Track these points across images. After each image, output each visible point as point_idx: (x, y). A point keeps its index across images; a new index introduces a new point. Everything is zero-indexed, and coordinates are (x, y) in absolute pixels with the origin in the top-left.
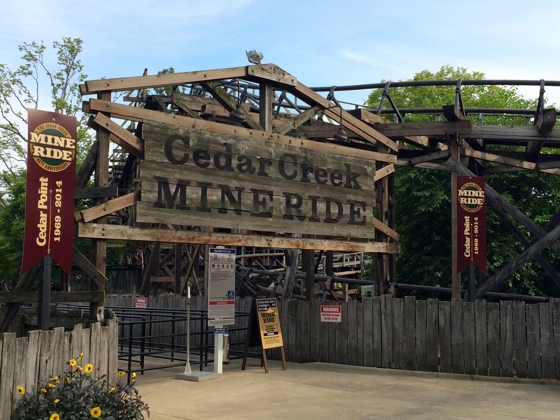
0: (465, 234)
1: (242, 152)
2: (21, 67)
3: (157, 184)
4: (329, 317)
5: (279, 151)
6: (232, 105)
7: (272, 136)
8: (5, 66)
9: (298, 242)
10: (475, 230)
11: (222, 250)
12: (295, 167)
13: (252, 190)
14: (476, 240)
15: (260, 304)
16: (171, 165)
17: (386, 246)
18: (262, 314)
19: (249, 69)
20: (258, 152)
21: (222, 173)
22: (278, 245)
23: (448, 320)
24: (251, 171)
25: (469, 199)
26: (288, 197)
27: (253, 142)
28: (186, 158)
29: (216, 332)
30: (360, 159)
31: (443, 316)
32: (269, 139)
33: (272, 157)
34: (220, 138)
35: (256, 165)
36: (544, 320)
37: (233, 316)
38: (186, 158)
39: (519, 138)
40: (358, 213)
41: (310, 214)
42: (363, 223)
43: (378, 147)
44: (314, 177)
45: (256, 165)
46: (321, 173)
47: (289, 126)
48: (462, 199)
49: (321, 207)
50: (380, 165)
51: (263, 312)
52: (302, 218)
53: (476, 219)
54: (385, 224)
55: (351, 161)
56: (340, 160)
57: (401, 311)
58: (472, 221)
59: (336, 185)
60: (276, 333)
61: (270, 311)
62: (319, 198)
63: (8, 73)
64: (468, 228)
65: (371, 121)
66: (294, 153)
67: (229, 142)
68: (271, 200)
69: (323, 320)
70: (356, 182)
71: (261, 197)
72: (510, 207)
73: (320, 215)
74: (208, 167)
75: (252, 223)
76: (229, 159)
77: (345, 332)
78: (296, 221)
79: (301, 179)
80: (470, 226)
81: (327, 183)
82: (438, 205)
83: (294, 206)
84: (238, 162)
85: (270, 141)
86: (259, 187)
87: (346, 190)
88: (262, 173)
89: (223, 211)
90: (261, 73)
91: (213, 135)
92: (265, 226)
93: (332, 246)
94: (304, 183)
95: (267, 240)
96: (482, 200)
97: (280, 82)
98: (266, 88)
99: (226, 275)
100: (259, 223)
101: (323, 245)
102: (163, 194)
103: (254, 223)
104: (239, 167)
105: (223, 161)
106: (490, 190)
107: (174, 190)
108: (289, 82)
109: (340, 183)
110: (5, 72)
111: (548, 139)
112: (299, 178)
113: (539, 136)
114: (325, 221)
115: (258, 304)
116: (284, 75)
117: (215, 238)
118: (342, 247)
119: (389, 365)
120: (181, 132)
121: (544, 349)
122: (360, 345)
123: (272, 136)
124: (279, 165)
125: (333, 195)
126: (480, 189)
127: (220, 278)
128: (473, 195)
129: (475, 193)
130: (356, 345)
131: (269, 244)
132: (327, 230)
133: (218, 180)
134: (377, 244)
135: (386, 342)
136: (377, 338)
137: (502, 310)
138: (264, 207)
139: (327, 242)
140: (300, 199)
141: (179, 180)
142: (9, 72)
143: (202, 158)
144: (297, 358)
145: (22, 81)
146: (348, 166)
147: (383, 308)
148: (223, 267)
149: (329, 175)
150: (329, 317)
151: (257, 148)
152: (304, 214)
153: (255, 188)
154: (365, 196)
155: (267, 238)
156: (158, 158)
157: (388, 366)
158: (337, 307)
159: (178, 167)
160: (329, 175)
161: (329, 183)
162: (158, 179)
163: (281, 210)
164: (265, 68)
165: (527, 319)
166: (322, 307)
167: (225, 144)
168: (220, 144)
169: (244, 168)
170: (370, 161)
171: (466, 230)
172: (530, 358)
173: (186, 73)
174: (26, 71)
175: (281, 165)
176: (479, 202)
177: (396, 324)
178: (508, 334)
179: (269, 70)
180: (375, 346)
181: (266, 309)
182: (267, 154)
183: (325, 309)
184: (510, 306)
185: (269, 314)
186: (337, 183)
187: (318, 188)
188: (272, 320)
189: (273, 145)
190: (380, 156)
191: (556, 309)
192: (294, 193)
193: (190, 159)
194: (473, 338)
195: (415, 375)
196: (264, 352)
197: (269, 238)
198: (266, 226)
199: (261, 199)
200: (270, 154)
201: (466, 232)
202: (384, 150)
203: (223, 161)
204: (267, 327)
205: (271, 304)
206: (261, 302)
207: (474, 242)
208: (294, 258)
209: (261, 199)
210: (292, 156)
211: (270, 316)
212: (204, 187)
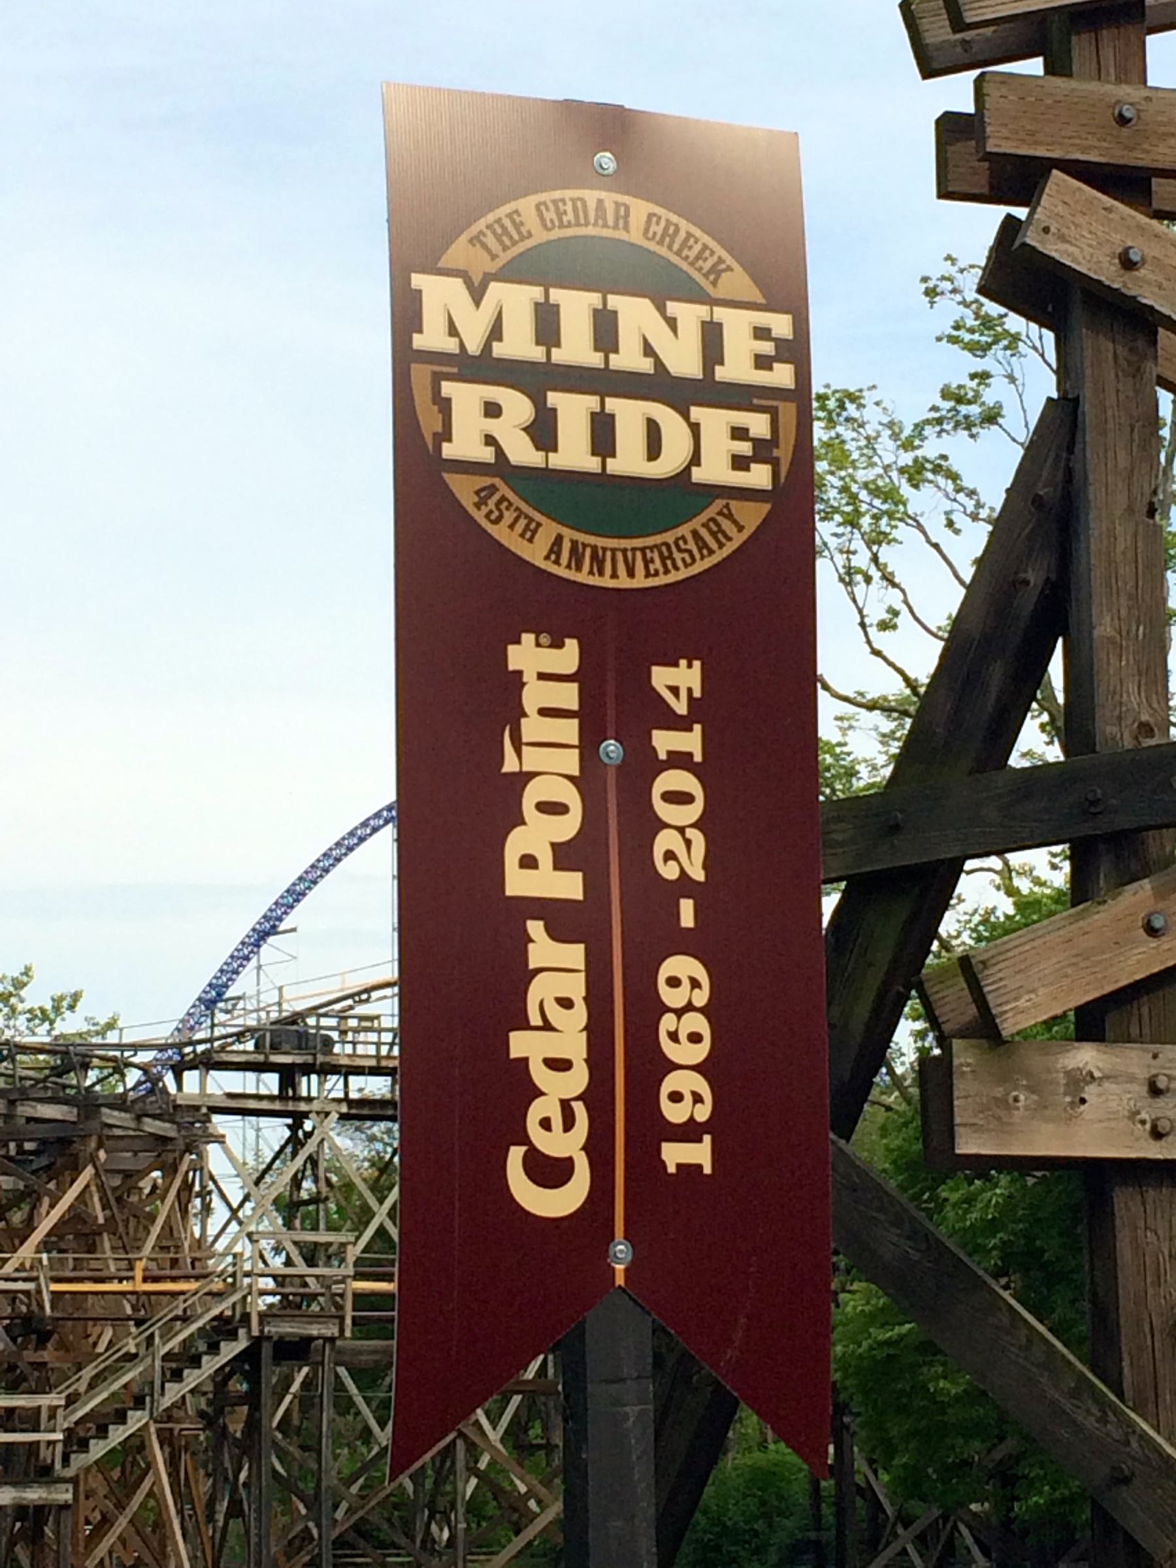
0: (518, 883)
10: (665, 841)
96: (759, 424)
128: (630, 358)
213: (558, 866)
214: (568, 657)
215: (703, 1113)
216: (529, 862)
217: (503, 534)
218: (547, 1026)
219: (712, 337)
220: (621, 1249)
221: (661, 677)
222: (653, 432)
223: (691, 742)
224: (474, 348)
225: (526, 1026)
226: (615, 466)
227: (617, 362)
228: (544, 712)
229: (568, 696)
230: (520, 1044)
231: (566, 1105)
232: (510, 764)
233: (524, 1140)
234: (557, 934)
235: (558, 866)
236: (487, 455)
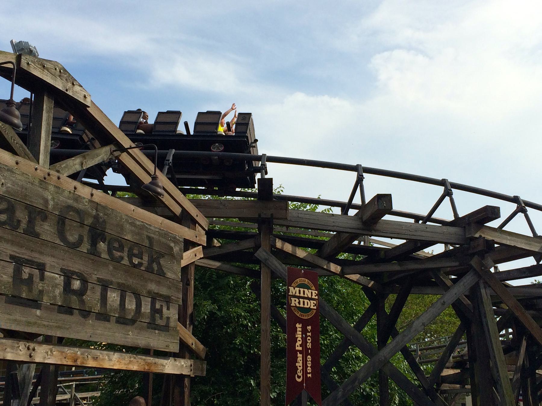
0: (297, 348)
5: (59, 200)
9: (76, 353)
10: (308, 344)
13: (12, 257)
17: (190, 365)
19: (22, 60)
22: (45, 358)
26: (68, 276)
32: (45, 178)
35: (22, 215)
40: (160, 311)
41: (97, 308)
42: (166, 328)
44: (106, 249)
45: (22, 215)
46: (116, 245)
47: (74, 165)
48: (293, 299)
49: (113, 297)
53: (309, 328)
54: (189, 331)
56: (141, 229)
58: (304, 331)
59: (135, 266)
62: (111, 283)
64: (299, 341)
66: (80, 206)
68: (42, 278)
70: (159, 264)
71: (26, 271)
75: (8, 316)
78: (76, 317)
79: (88, 250)
80: (302, 338)
81: (122, 262)
82: (206, 317)
83: (74, 292)
86: (24, 254)
87: (147, 275)
88: (30, 232)
92: (29, 324)
93: (123, 362)
94: (92, 257)
95: (28, 349)
96: (315, 302)
97: (68, 93)
98: (45, 98)
100: (18, 316)
103: (11, 317)
108: (80, 98)
109: (140, 264)
112: (85, 248)
113: (363, 229)
116: (73, 84)
118: (137, 364)
123: (49, 175)
124: (58, 223)
125: (131, 281)
126: (313, 288)
128: (306, 296)
129: (308, 293)
131: (31, 356)
134: (180, 362)
138: (30, 290)
139: (116, 356)
140: (84, 281)
149: (126, 249)
151: (26, 189)
152: (88, 306)
153: (18, 255)
154: (169, 288)
160: (126, 249)
161: (126, 262)
163: (55, 296)
164: (48, 65)
171: (299, 343)
175: (61, 222)
176: (312, 305)
179: (53, 71)
182: (42, 202)
186: (136, 263)
187: (111, 268)
189: (51, 188)
192: (77, 271)
199: (25, 276)
200: (46, 201)
207: (306, 361)
208: (26, 387)
209: (25, 276)
210: (78, 211)
213: (300, 347)
214: (300, 326)
217: (296, 313)
218: (299, 363)
221: (308, 327)
224: (294, 294)
225: (297, 363)
228: (299, 331)
231: (300, 370)
233: (297, 374)
234: (300, 354)
235: (300, 347)
236: (295, 305)
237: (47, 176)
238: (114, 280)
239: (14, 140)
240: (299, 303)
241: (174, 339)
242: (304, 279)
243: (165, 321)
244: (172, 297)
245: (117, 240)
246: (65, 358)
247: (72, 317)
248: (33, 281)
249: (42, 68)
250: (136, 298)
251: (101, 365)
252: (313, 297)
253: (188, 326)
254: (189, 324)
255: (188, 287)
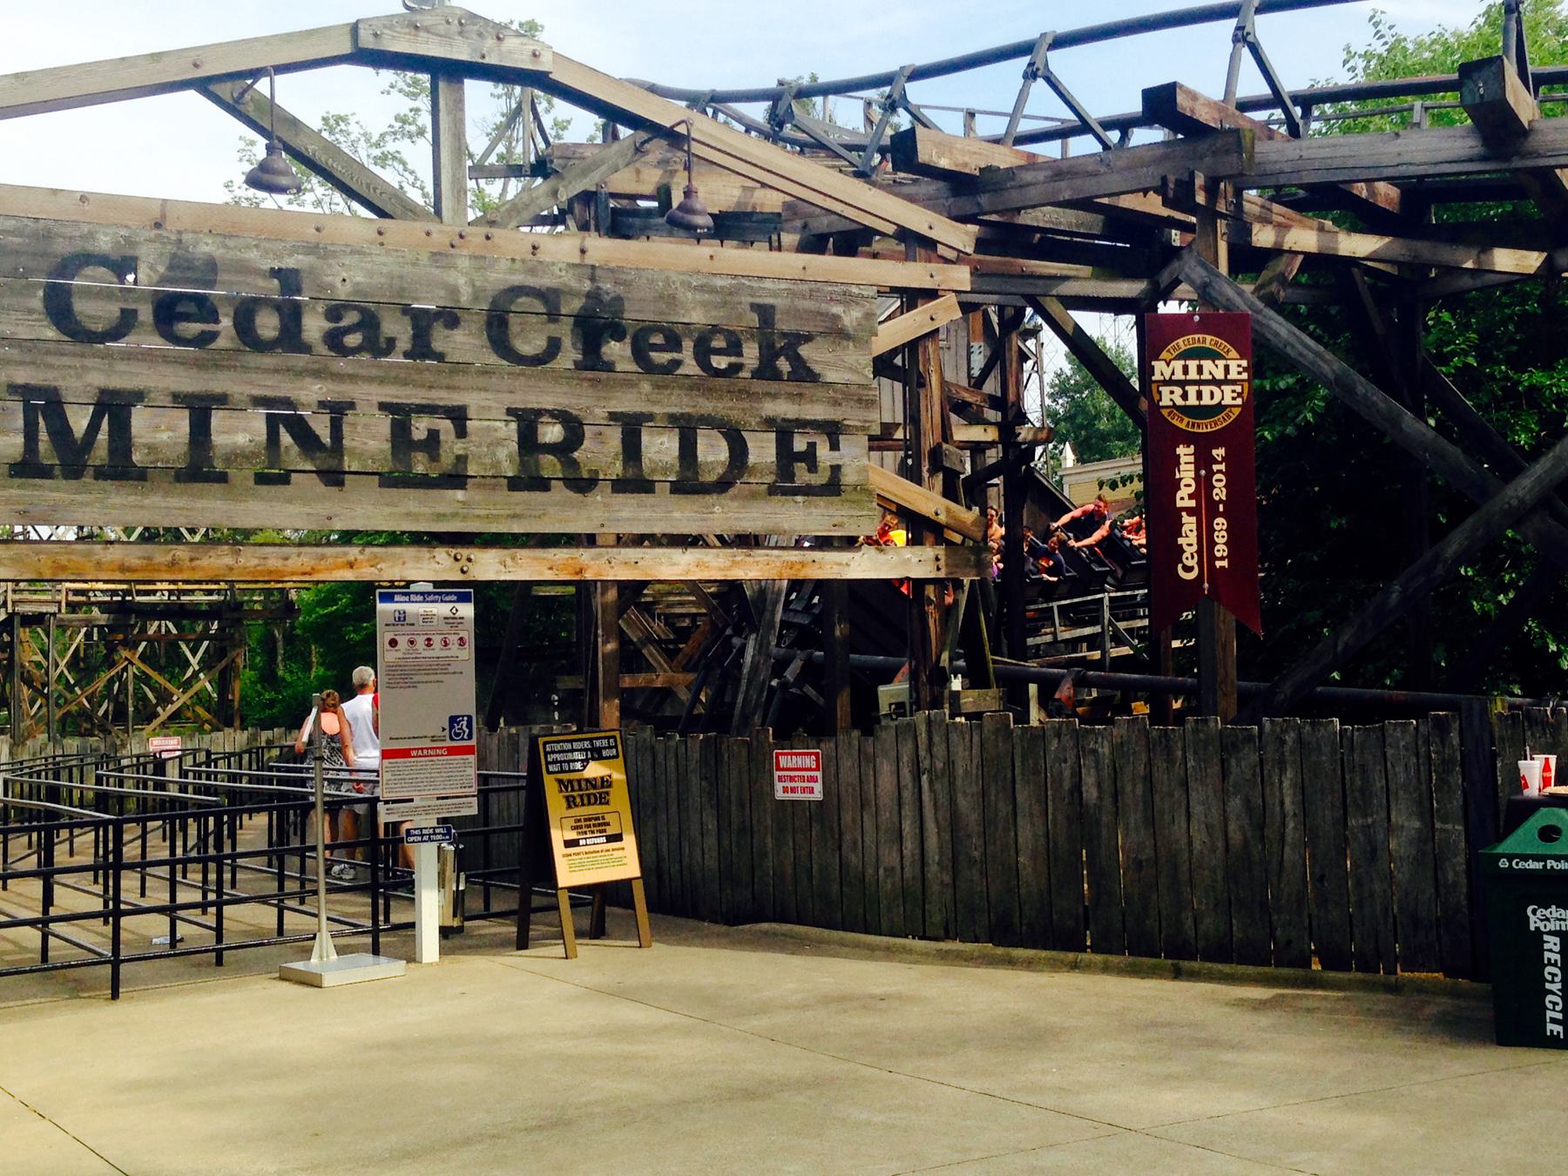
0: (1179, 504)
1: (343, 292)
2: (397, 118)
3: (19, 406)
4: (793, 784)
5: (487, 280)
6: (311, 148)
7: (461, 236)
8: (352, 120)
11: (422, 594)
12: (552, 326)
14: (1220, 523)
15: (553, 752)
16: (69, 348)
18: (560, 782)
20: (403, 289)
21: (268, 360)
23: (1107, 785)
24: (378, 346)
25: (1192, 390)
26: (527, 421)
27: (382, 259)
28: (125, 324)
29: (412, 839)
30: (813, 286)
31: (1093, 771)
32: (453, 246)
33: (459, 301)
34: (253, 255)
35: (397, 329)
36: (1402, 777)
37: (474, 790)
38: (125, 324)
39: (1421, 170)
40: (810, 457)
41: (617, 470)
42: (833, 487)
43: (915, 244)
44: (628, 352)
45: (397, 329)
46: (658, 339)
48: (1165, 390)
50: (912, 297)
51: (565, 777)
52: (583, 484)
53: (1219, 452)
54: (931, 488)
55: (775, 294)
57: (975, 762)
58: (1203, 461)
59: (718, 373)
60: (617, 838)
61: (595, 770)
62: (650, 417)
63: (363, 139)
65: (966, 165)
66: (544, 281)
67: (290, 263)
68: (461, 432)
69: (780, 795)
70: (798, 361)
71: (420, 427)
72: (1382, 405)
73: (653, 471)
74: (213, 346)
75: (387, 510)
76: (292, 316)
77: (832, 829)
79: (576, 363)
80: (1197, 478)
82: (1309, 416)
83: (551, 448)
84: (328, 325)
85: (452, 251)
87: (759, 386)
89: (273, 477)
90: (409, 41)
91: (225, 246)
92: (440, 517)
94: (589, 374)
96: (1238, 389)
97: (487, 61)
99: (442, 667)
101: (674, 564)
102: (43, 436)
103: (396, 510)
104: (334, 340)
105: (268, 325)
106: (1317, 354)
107: (85, 423)
108: (522, 61)
109: (734, 369)
110: (353, 137)
111: (1518, 163)
112: (569, 356)
114: (678, 488)
115: (546, 754)
116: (499, 39)
117: (256, 562)
119: (946, 930)
120: (104, 243)
121: (1402, 874)
122: (870, 871)
123: (461, 236)
125: (706, 406)
126: (1234, 354)
127: (416, 678)
128: (1206, 376)
129: (1213, 369)
130: (860, 869)
131: (463, 572)
132: (683, 515)
133: (251, 383)
135: (937, 858)
136: (910, 846)
137: (1271, 748)
138: (434, 457)
141: (103, 392)
142: (365, 135)
143: (188, 318)
144: (724, 910)
145: (404, 156)
146: (766, 313)
147: (922, 753)
148: (429, 645)
149: (688, 345)
150: (793, 784)
151: (401, 277)
152: (590, 471)
153: (395, 401)
155: (453, 552)
156: (20, 329)
157: (942, 933)
158: (810, 754)
159: (99, 349)
160: (688, 345)
161: (690, 367)
162: (25, 392)
163: (499, 462)
165: (1347, 777)
166: (777, 755)
167: (276, 273)
168: (257, 272)
169: (353, 340)
170: (855, 290)
171: (1184, 492)
172: (1360, 904)
173: (123, 59)
174: (413, 128)
176: (1228, 395)
177: (963, 803)
178: (1291, 825)
180: (908, 873)
181: (578, 766)
182: (442, 293)
183: (783, 761)
184: (1292, 735)
185: (587, 780)
186: (723, 366)
188: (603, 800)
189: (464, 263)
190: (914, 274)
191: (1437, 740)
193: (142, 324)
194: (1184, 841)
195: (1011, 963)
196: (564, 901)
197: (464, 552)
198: (444, 515)
200: (454, 291)
201: (1184, 498)
202: (920, 252)
203: (268, 325)
204: (579, 821)
205: (599, 750)
206: (558, 747)
207: (1211, 530)
211: (595, 787)
212: (200, 409)
215: (1225, 554)
216: (1182, 499)
217: (1175, 422)
219: (1227, 368)
220: (1206, 585)
221: (1214, 452)
222: (1212, 393)
223: (1222, 467)
226: (1202, 403)
227: (1203, 377)
229: (1192, 459)
230: (1180, 541)
232: (1177, 476)
234: (1189, 515)
236: (1171, 404)
237: (457, 241)
238: (657, 410)
239: (375, 189)
240: (1185, 396)
241: (863, 509)
242: (1201, 336)
243: (828, 473)
244: (846, 422)
245: (656, 328)
246: (551, 568)
247: (548, 494)
248: (439, 442)
249: (413, 31)
250: (726, 436)
251: (647, 574)
252: (1233, 375)
253: (926, 475)
254: (928, 471)
255: (922, 392)
